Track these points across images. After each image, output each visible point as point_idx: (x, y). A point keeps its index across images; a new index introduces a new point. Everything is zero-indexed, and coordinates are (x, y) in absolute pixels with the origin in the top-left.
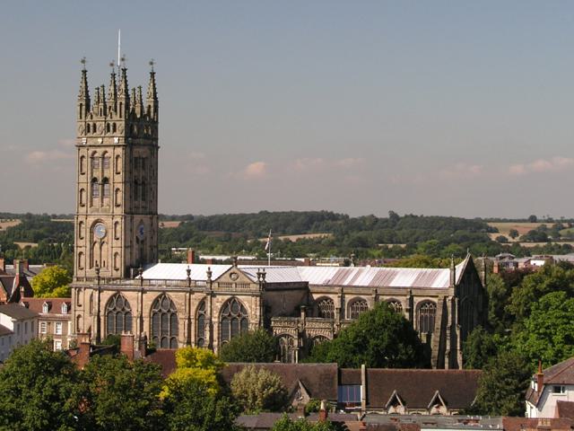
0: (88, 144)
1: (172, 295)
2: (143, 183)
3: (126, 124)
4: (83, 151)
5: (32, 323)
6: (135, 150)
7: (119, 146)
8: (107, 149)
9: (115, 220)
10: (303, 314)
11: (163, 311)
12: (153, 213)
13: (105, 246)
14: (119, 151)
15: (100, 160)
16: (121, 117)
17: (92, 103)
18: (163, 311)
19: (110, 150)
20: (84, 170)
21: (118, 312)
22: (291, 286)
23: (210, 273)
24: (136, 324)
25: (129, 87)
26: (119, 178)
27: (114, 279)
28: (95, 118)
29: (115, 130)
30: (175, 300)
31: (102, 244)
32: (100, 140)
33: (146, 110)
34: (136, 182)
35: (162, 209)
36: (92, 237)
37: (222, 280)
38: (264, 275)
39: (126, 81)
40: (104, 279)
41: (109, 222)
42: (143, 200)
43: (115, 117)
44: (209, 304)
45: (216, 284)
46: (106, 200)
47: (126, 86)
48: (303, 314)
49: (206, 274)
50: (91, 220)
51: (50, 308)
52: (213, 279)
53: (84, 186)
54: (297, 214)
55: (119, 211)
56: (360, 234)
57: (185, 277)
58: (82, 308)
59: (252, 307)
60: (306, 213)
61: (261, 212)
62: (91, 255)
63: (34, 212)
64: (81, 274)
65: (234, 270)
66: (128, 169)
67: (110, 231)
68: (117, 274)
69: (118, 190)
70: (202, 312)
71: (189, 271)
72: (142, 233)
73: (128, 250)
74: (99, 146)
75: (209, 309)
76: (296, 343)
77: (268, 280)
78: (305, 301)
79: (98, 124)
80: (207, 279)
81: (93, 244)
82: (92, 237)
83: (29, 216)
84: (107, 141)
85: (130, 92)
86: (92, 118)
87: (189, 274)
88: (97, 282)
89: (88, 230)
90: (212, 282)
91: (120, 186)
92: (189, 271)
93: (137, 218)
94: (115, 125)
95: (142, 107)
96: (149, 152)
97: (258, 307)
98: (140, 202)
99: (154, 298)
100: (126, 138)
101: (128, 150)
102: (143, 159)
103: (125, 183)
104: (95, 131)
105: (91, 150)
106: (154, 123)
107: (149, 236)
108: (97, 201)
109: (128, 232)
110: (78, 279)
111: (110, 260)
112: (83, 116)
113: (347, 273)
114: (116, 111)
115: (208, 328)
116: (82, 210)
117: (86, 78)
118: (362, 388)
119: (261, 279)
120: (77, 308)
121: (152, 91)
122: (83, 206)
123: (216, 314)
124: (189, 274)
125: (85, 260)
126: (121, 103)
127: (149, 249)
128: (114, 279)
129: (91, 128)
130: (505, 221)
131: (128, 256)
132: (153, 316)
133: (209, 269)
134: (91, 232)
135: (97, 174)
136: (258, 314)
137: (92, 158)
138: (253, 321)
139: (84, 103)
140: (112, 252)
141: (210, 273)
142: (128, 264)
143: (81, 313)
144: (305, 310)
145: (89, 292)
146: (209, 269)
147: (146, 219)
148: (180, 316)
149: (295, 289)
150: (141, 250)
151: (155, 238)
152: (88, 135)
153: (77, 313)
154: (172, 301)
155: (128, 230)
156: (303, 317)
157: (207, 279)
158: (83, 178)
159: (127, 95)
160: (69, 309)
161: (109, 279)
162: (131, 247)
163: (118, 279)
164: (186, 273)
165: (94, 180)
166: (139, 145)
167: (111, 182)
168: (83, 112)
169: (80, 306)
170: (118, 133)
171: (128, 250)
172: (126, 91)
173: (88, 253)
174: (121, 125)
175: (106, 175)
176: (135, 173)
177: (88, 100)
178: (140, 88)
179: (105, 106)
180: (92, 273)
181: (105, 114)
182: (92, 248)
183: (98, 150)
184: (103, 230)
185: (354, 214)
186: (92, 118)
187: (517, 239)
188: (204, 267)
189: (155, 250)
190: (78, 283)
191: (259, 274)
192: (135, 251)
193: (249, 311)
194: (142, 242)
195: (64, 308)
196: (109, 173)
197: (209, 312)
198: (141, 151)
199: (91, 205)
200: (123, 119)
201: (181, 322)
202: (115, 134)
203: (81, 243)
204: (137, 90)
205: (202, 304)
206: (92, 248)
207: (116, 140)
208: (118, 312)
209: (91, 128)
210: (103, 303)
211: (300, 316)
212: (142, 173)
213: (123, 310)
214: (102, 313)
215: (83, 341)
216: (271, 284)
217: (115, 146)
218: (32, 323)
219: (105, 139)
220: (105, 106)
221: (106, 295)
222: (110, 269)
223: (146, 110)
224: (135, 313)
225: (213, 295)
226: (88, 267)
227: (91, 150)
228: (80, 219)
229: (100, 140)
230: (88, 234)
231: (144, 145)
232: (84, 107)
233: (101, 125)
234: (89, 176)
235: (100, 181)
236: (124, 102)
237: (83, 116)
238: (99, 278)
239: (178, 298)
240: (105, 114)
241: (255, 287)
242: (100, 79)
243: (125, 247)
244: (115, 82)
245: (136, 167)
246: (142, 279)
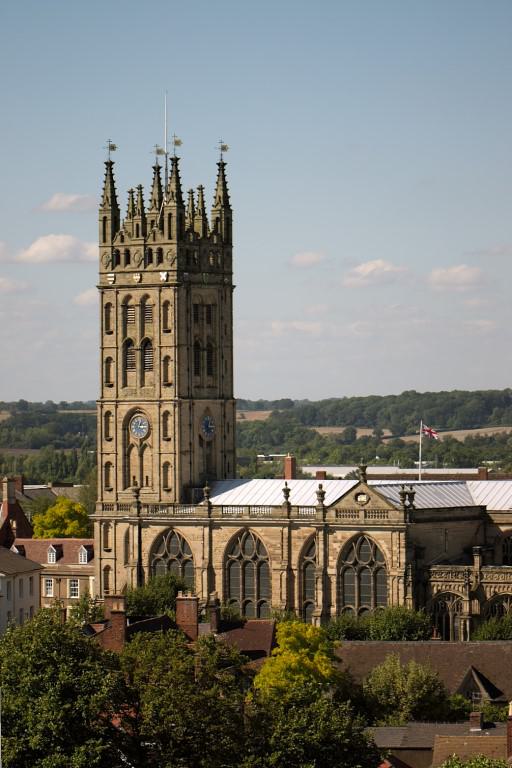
0: (118, 283)
1: (258, 531)
2: (209, 345)
3: (180, 250)
4: (110, 296)
5: (31, 579)
6: (195, 291)
7: (169, 286)
9: (163, 410)
10: (477, 559)
11: (244, 556)
12: (226, 396)
13: (147, 453)
14: (169, 294)
15: (138, 309)
16: (170, 238)
17: (123, 215)
18: (244, 556)
19: (153, 293)
20: (113, 327)
22: (458, 513)
23: (321, 495)
24: (200, 581)
25: (182, 189)
26: (169, 339)
27: (163, 507)
28: (128, 241)
29: (160, 260)
30: (264, 540)
32: (137, 277)
33: (211, 225)
34: (197, 345)
35: (245, 387)
36: (126, 438)
37: (342, 505)
38: (412, 496)
39: (178, 179)
40: (146, 506)
41: (153, 412)
42: (210, 373)
43: (162, 239)
44: (321, 546)
45: (332, 513)
46: (148, 374)
47: (179, 186)
48: (477, 559)
49: (316, 496)
50: (124, 409)
51: (59, 556)
52: (327, 503)
53: (112, 353)
54: (466, 395)
55: (169, 393)
57: (280, 500)
58: (112, 554)
59: (391, 548)
60: (478, 394)
61: (406, 394)
63: (32, 399)
64: (109, 498)
66: (183, 323)
67: (155, 427)
68: (168, 498)
69: (167, 358)
70: (309, 559)
71: (287, 492)
72: (208, 430)
73: (186, 459)
74: (135, 287)
75: (321, 554)
76: (466, 608)
77: (419, 503)
78: (480, 538)
79: (133, 250)
80: (317, 503)
81: (128, 448)
82: (126, 438)
83: (23, 405)
84: (148, 278)
85: (185, 197)
86: (122, 240)
87: (287, 496)
88: (135, 511)
89: (120, 426)
90: (325, 509)
91: (171, 352)
92: (287, 492)
93: (200, 405)
94: (160, 251)
95: (205, 220)
96: (215, 292)
97: (403, 550)
98: (207, 380)
99: (230, 535)
100: (180, 272)
101: (183, 292)
102: (208, 306)
103: (178, 346)
104: (128, 262)
105: (123, 294)
106: (227, 243)
107: (218, 432)
109: (186, 429)
110: (106, 507)
111: (156, 476)
112: (109, 238)
114: (162, 228)
115: (320, 586)
116: (110, 393)
117: (112, 175)
119: (407, 503)
120: (105, 555)
121: (221, 193)
122: (111, 386)
123: (333, 562)
124: (287, 496)
125: (116, 476)
126: (170, 215)
127: (219, 455)
128: (163, 507)
129: (122, 257)
131: (186, 468)
132: (228, 565)
133: (321, 486)
134: (126, 428)
135: (134, 333)
136: (403, 560)
137: (126, 307)
138: (395, 573)
139: (109, 216)
141: (321, 495)
142: (186, 480)
143: (111, 563)
144: (480, 552)
145: (122, 527)
146: (321, 486)
147: (215, 407)
148: (274, 565)
149: (465, 519)
150: (208, 458)
151: (230, 437)
152: (118, 268)
153: (105, 563)
154: (259, 541)
156: (477, 566)
157: (317, 503)
158: (110, 340)
159: (180, 201)
160: (91, 557)
161: (156, 507)
162: (191, 452)
163: (169, 505)
164: (283, 494)
165: (128, 343)
166: (201, 283)
167: (156, 345)
168: (109, 230)
169: (109, 551)
170: (166, 265)
171: (186, 459)
172: (179, 193)
173: (120, 464)
174: (171, 249)
175: (148, 334)
176: (195, 330)
178: (201, 189)
179: (144, 220)
180: (127, 496)
181: (144, 234)
182: (127, 456)
184: (144, 427)
186: (122, 240)
189: (230, 458)
190: (107, 514)
191: (403, 495)
192: (198, 459)
193: (389, 556)
194: (209, 444)
197: (321, 558)
198: (206, 294)
199: (125, 385)
200: (175, 241)
201: (275, 576)
202: (161, 267)
203: (109, 447)
204: (197, 192)
205: (309, 547)
206: (127, 456)
207: (163, 276)
209: (122, 257)
210: (147, 546)
211: (472, 564)
212: (207, 331)
213: (180, 556)
214: (145, 562)
215: (115, 608)
216: (423, 510)
217: (161, 287)
218: (31, 579)
219: (145, 275)
220: (144, 220)
221: (151, 534)
222: (157, 489)
223: (211, 225)
224: (199, 562)
225: (328, 530)
226: (120, 487)
227: (123, 294)
228: (106, 408)
229: (137, 277)
230: (120, 432)
231: (209, 284)
232: (109, 223)
233: (137, 252)
234: (120, 336)
235: (138, 344)
236: (175, 214)
237: (109, 238)
238: (139, 506)
239: (269, 537)
240: (144, 234)
241: (397, 517)
242: (135, 176)
243: (181, 452)
244: (159, 179)
245: (196, 319)
246: (210, 507)
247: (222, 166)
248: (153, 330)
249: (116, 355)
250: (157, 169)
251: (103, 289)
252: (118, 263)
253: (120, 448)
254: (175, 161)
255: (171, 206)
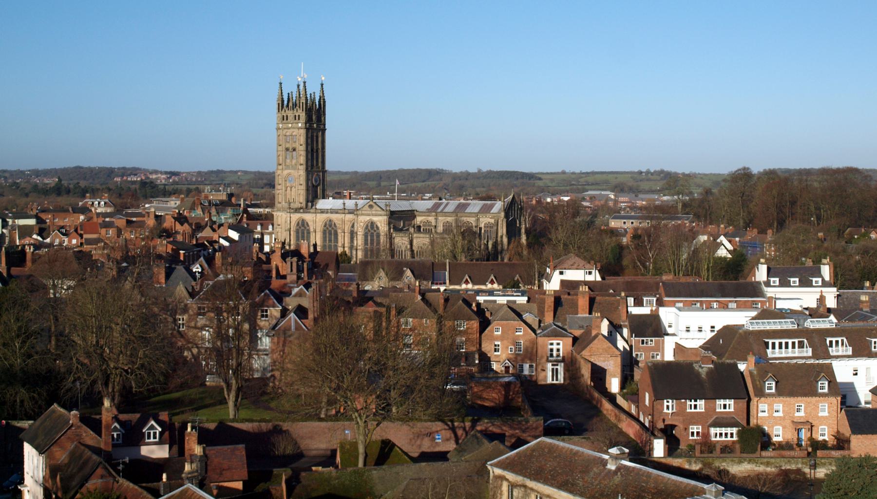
13: (293, 189)
19: (296, 130)
21: (303, 229)
23: (356, 205)
25: (308, 94)
35: (329, 167)
56: (460, 182)
62: (286, 195)
63: (203, 170)
65: (371, 203)
85: (308, 96)
108: (288, 161)
113: (441, 204)
116: (280, 167)
118: (447, 273)
130: (548, 173)
140: (299, 194)
148: (339, 231)
155: (308, 180)
165: (287, 149)
174: (303, 115)
177: (283, 101)
185: (456, 167)
187: (554, 184)
188: (353, 201)
195: (270, 227)
196: (297, 145)
208: (303, 229)
217: (299, 128)
224: (312, 230)
233: (291, 118)
250: (298, 86)
251: (278, 129)
254: (305, 83)
255: (303, 100)
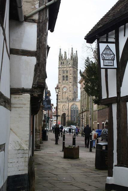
8: (67, 68)
13: (66, 93)
19: (68, 69)
31: (65, 93)
32: (65, 66)
36: (63, 91)
79: (65, 62)
82: (63, 91)
85: (74, 54)
104: (64, 64)
116: (60, 84)
143: (60, 111)
152: (62, 65)
158: (60, 76)
183: (64, 68)
200: (72, 60)
209: (63, 63)
217: (70, 67)
247: (72, 48)
248: (68, 74)
249: (62, 78)
251: (59, 68)
252: (62, 64)
253: (62, 93)
